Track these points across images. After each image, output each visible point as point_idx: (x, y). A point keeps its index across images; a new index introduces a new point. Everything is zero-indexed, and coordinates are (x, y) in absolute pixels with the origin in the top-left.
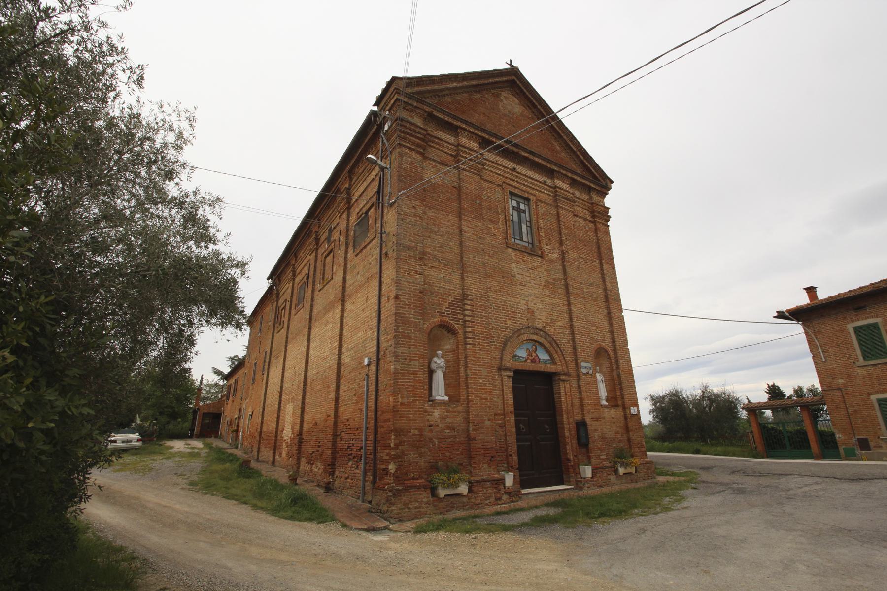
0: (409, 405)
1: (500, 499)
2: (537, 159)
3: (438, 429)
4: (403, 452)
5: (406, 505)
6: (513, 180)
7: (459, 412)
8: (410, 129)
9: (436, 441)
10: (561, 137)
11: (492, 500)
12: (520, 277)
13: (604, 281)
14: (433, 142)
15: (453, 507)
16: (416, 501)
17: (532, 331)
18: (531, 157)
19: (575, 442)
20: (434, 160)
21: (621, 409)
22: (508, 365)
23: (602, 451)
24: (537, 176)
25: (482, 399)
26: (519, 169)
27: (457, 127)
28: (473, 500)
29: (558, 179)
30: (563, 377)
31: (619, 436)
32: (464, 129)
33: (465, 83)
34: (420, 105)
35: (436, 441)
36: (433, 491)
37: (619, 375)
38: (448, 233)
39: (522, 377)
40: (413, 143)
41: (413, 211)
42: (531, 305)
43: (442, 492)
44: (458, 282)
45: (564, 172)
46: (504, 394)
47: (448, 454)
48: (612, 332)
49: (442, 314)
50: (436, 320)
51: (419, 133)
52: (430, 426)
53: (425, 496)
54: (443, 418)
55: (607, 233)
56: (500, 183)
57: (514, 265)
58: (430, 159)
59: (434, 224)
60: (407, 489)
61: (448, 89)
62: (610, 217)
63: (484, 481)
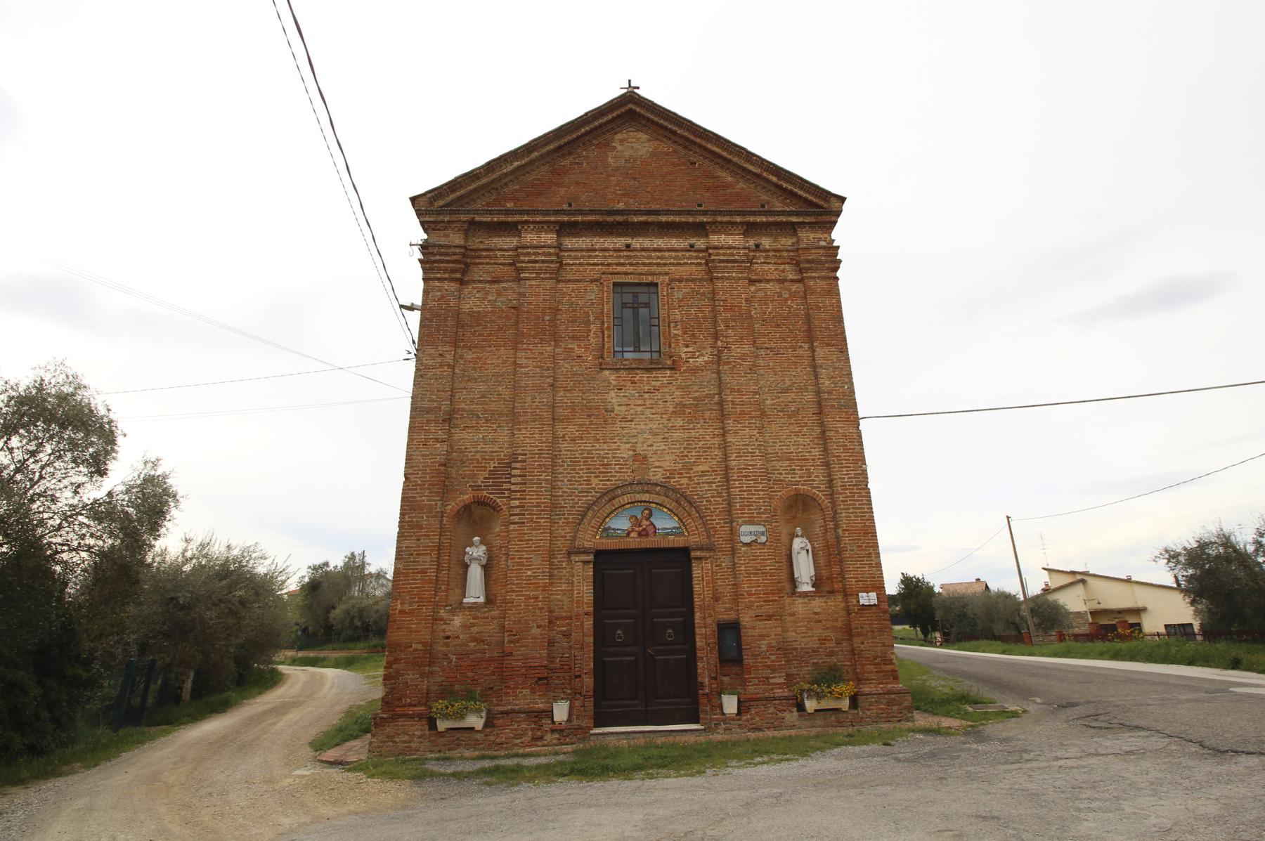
0: (411, 612)
1: (541, 738)
2: (664, 219)
3: (457, 642)
4: (397, 671)
5: (390, 738)
6: (623, 265)
7: (493, 618)
8: (441, 255)
9: (454, 658)
10: (730, 161)
11: (527, 739)
12: (623, 408)
13: (816, 375)
14: (479, 257)
15: (459, 745)
16: (405, 733)
17: (638, 488)
18: (652, 218)
19: (714, 658)
20: (480, 282)
21: (840, 598)
22: (587, 544)
23: (774, 671)
24: (674, 242)
25: (528, 598)
26: (637, 243)
27: (516, 224)
28: (492, 738)
29: (715, 233)
30: (699, 554)
31: (831, 645)
32: (527, 222)
33: (536, 154)
34: (455, 218)
35: (454, 658)
36: (432, 724)
37: (838, 538)
38: (496, 375)
39: (608, 563)
40: (445, 271)
42: (640, 449)
43: (442, 725)
44: (507, 439)
45: (726, 219)
46: (579, 586)
47: (470, 674)
48: (827, 465)
49: (477, 488)
50: (467, 497)
51: (455, 254)
52: (448, 638)
53: (418, 728)
54: (465, 627)
55: (834, 292)
56: (596, 276)
57: (612, 394)
58: (474, 282)
59: (474, 369)
60: (394, 718)
61: (506, 175)
62: (840, 261)
63: (513, 711)
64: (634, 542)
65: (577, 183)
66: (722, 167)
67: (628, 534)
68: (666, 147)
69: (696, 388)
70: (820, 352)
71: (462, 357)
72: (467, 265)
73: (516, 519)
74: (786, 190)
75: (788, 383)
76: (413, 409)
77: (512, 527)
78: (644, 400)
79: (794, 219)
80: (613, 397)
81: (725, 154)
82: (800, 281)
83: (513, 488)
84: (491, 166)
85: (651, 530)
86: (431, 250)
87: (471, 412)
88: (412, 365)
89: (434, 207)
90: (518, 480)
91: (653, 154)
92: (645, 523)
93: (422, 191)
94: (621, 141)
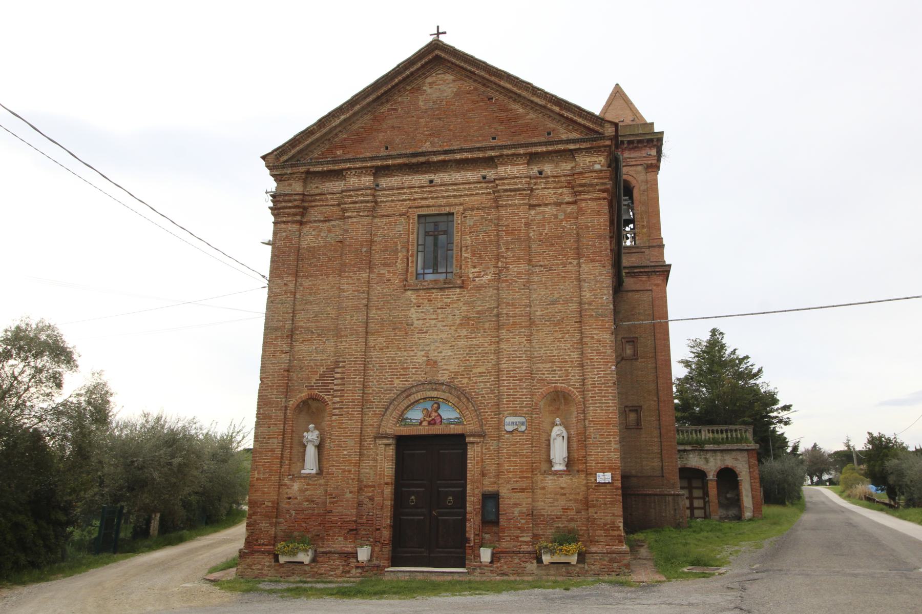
0: (264, 480)
1: (349, 572)
2: (458, 156)
3: (296, 501)
4: (255, 521)
6: (426, 199)
7: (320, 485)
8: (285, 201)
10: (519, 96)
11: (339, 572)
12: (421, 322)
14: (314, 201)
17: (428, 387)
20: (315, 221)
21: (583, 476)
22: (389, 431)
25: (344, 471)
26: (438, 178)
27: (341, 171)
29: (503, 164)
30: (471, 439)
32: (349, 169)
33: (357, 107)
34: (295, 170)
38: (326, 298)
40: (289, 215)
41: (284, 288)
42: (432, 355)
43: (282, 559)
44: (333, 349)
45: (512, 151)
46: (382, 463)
47: (304, 525)
49: (311, 388)
50: (304, 395)
51: (295, 200)
52: (290, 498)
53: (267, 561)
54: (301, 490)
56: (404, 210)
57: (413, 310)
58: (310, 222)
59: (310, 294)
60: (252, 553)
61: (336, 127)
63: (330, 552)
64: (425, 430)
65: (393, 127)
66: (515, 100)
67: (421, 423)
68: (468, 85)
69: (479, 303)
70: (585, 268)
71: (301, 285)
72: (305, 208)
73: (337, 411)
74: (567, 118)
75: (556, 296)
76: (266, 328)
77: (334, 418)
78: (437, 314)
79: (572, 147)
80: (413, 313)
81: (515, 89)
82: (575, 202)
83: (336, 388)
84: (322, 122)
85: (438, 420)
86: (278, 199)
87: (308, 329)
88: (267, 289)
89: (281, 161)
90: (339, 381)
91: (457, 94)
92: (434, 414)
93: (270, 151)
94: (430, 84)
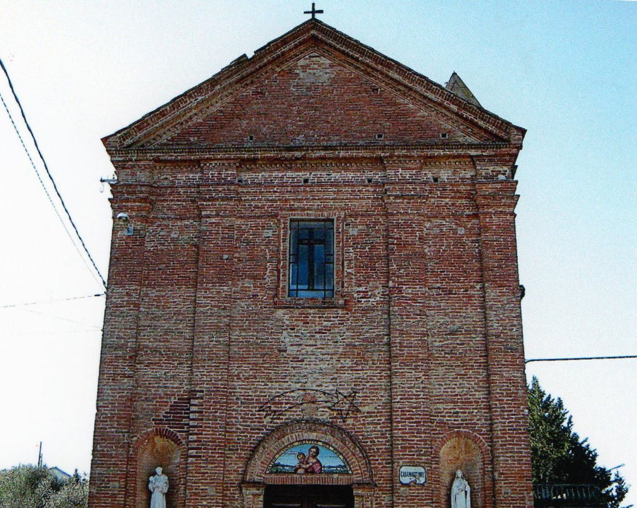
10: (410, 89)
12: (295, 348)
38: (178, 313)
41: (126, 299)
64: (300, 479)
65: (259, 114)
66: (404, 94)
67: (296, 470)
68: (349, 71)
69: (366, 328)
70: (492, 293)
71: (147, 295)
72: (152, 203)
73: (193, 452)
74: (466, 119)
75: (458, 324)
76: (103, 346)
77: (190, 460)
78: (316, 340)
79: (473, 153)
80: (286, 338)
81: (406, 82)
82: (476, 216)
83: (191, 423)
84: (176, 102)
85: (317, 469)
86: (119, 189)
87: (155, 350)
88: (102, 300)
89: (123, 146)
90: (196, 416)
91: (334, 81)
92: (313, 460)
93: (113, 132)
94: (305, 68)
